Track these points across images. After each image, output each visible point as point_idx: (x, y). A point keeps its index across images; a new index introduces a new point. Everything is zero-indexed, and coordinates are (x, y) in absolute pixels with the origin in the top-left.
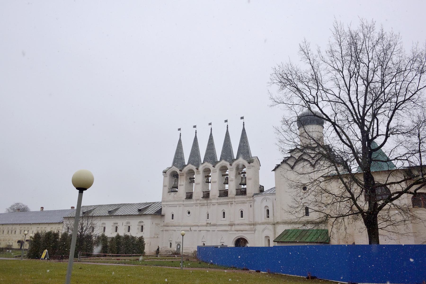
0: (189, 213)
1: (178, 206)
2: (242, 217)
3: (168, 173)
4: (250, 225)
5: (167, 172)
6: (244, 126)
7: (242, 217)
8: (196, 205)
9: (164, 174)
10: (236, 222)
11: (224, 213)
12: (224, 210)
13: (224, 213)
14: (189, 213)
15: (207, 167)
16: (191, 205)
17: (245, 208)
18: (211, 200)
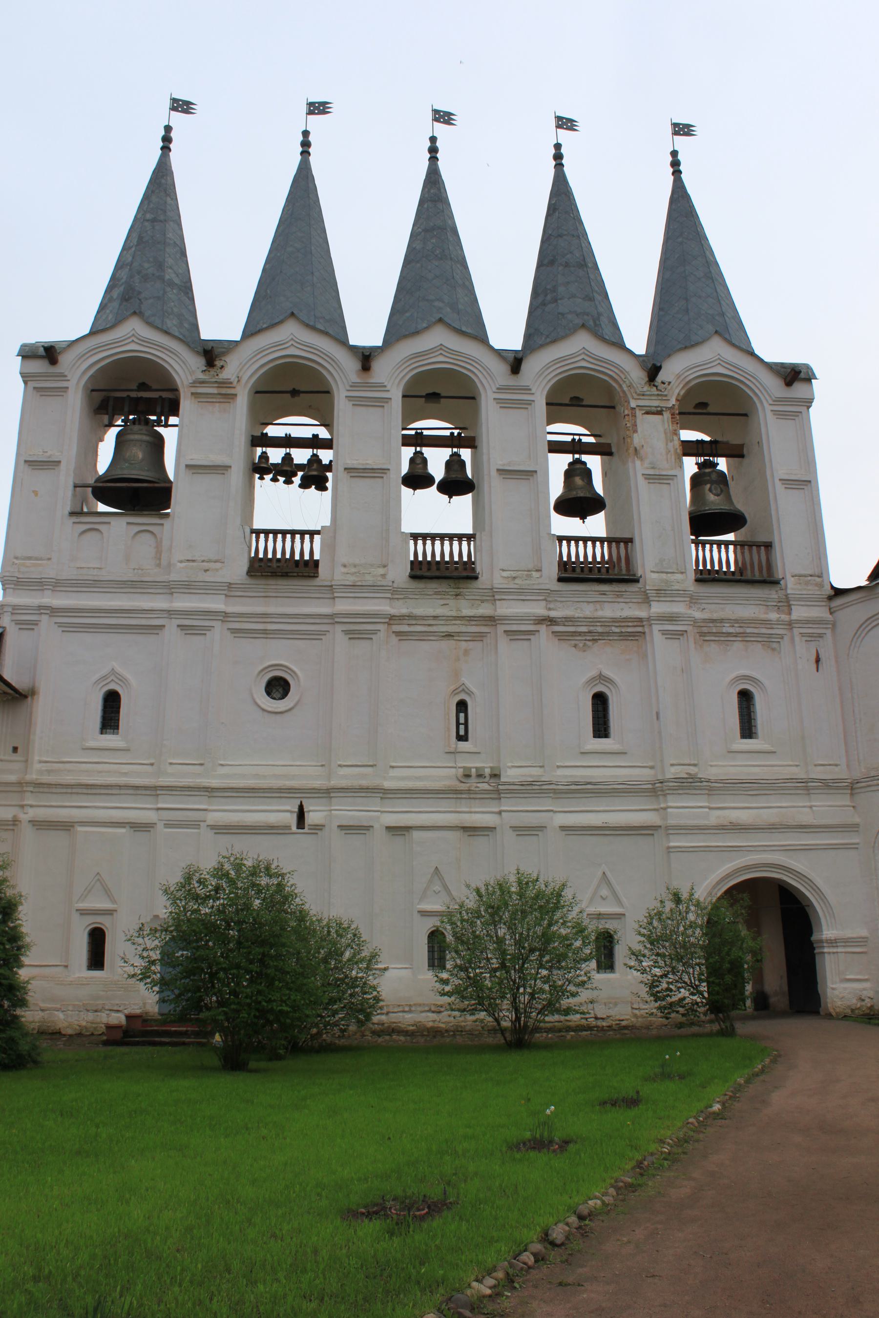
0: (278, 687)
1: (171, 626)
2: (748, 730)
3: (76, 374)
4: (827, 786)
5: (66, 360)
6: (677, 173)
7: (748, 730)
8: (358, 629)
9: (39, 366)
10: (716, 769)
11: (600, 702)
12: (601, 678)
13: (600, 702)
14: (278, 687)
15: (439, 361)
16: (310, 630)
17: (775, 675)
18: (493, 595)
